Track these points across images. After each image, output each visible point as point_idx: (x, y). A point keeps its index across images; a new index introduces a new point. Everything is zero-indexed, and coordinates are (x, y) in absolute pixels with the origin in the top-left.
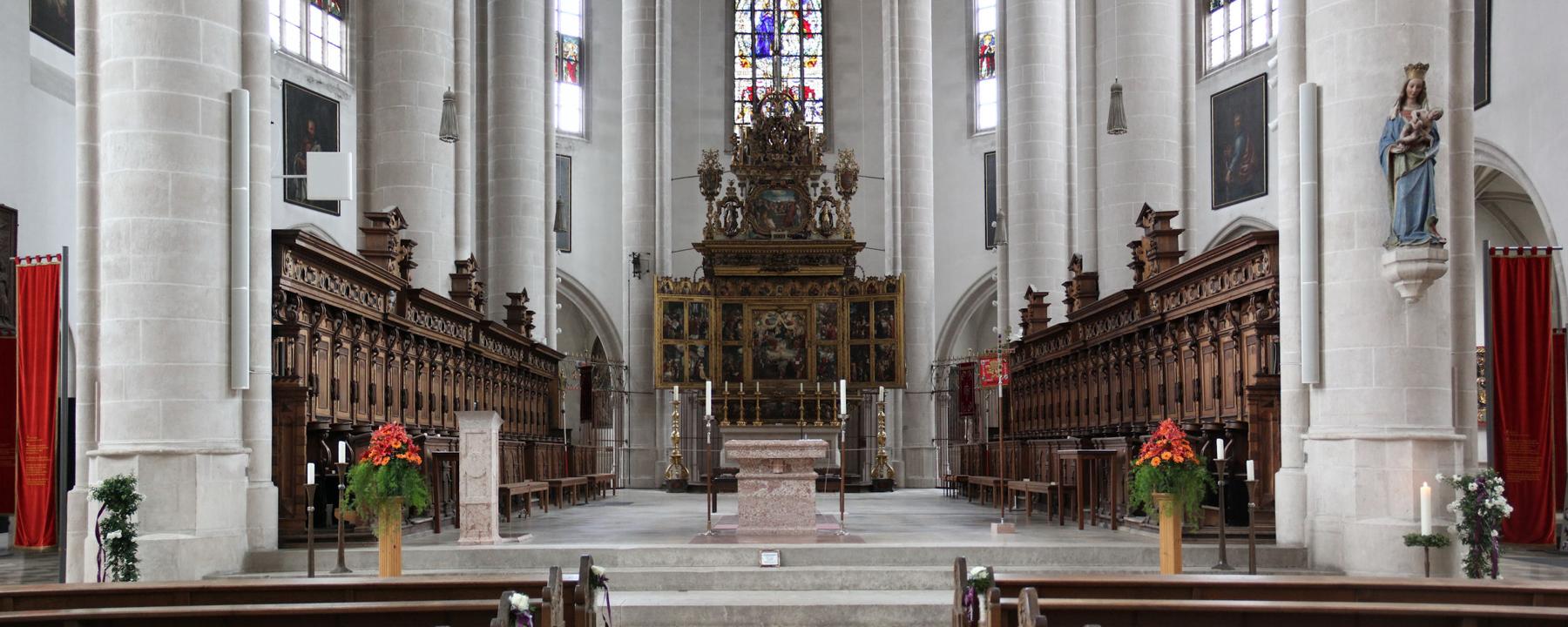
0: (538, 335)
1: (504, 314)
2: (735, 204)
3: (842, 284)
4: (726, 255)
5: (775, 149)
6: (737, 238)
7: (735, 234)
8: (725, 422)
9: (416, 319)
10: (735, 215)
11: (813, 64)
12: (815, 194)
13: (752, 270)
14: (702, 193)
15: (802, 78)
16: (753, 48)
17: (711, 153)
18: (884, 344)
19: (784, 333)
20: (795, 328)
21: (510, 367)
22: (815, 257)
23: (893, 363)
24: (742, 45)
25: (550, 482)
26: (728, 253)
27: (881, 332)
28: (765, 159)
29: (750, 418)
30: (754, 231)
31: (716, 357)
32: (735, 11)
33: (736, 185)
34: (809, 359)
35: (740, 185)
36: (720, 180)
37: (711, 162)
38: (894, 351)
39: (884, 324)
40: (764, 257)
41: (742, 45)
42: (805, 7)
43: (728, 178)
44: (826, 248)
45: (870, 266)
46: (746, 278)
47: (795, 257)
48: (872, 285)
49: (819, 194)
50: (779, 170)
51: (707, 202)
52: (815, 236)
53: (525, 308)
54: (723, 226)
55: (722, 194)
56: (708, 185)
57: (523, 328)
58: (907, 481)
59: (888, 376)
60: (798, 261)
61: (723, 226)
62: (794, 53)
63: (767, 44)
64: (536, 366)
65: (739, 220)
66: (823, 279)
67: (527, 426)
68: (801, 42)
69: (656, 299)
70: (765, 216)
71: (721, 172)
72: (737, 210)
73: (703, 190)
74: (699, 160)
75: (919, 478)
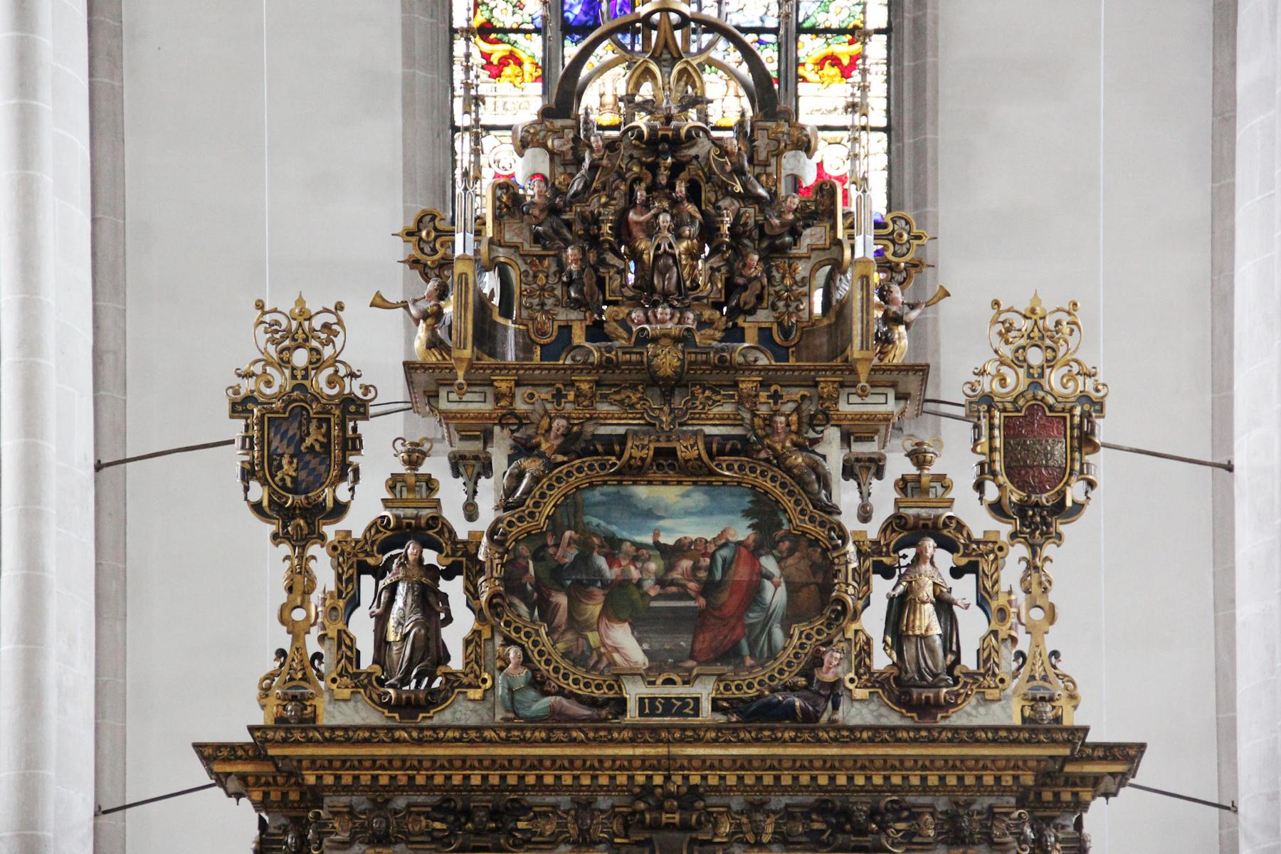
2: (430, 557)
4: (380, 798)
6: (444, 717)
7: (433, 700)
14: (257, 508)
22: (861, 807)
26: (394, 788)
28: (596, 332)
30: (538, 684)
33: (437, 466)
35: (457, 464)
36: (353, 444)
37: (300, 358)
40: (585, 807)
44: (926, 765)
47: (757, 807)
49: (884, 507)
51: (285, 549)
54: (366, 662)
56: (288, 468)
61: (366, 662)
65: (454, 637)
70: (594, 609)
71: (355, 407)
72: (444, 585)
73: (258, 492)
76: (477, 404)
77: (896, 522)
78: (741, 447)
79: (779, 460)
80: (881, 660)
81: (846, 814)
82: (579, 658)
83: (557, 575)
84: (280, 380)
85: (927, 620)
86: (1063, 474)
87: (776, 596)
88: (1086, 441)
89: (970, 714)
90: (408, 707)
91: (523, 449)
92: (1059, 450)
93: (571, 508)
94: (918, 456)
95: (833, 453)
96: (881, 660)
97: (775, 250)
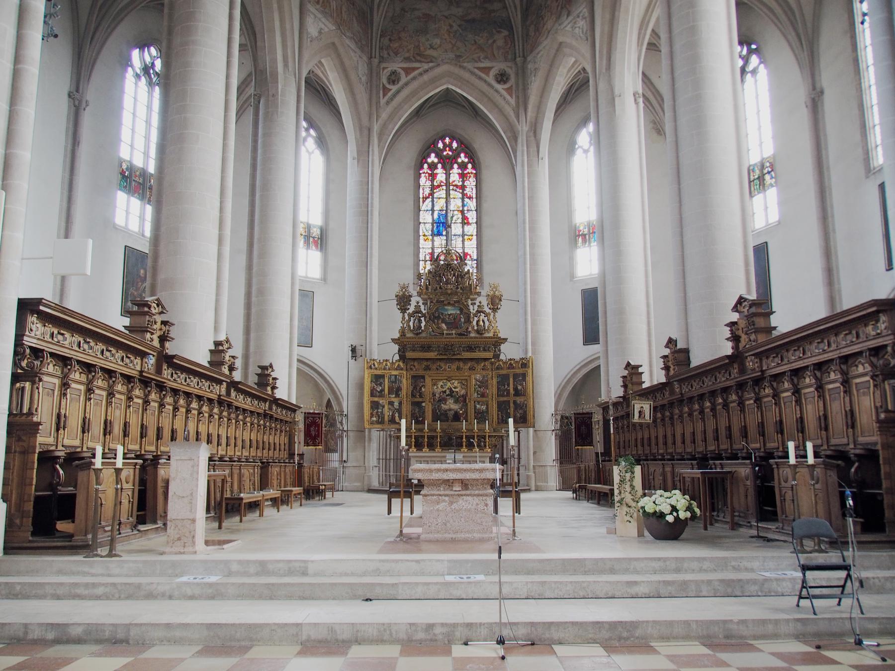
0: (281, 393)
1: (256, 379)
3: (492, 363)
5: (447, 283)
6: (420, 335)
7: (420, 333)
8: (413, 449)
9: (209, 388)
10: (420, 321)
11: (471, 240)
12: (473, 309)
13: (432, 355)
15: (463, 247)
16: (432, 230)
17: (404, 285)
18: (519, 400)
19: (451, 394)
20: (460, 390)
21: (258, 413)
23: (525, 412)
24: (426, 228)
25: (282, 491)
27: (517, 393)
29: (431, 447)
30: (433, 331)
31: (406, 408)
32: (420, 210)
33: (420, 304)
34: (469, 411)
36: (410, 301)
39: (519, 387)
41: (426, 228)
42: (466, 208)
43: (414, 301)
45: (508, 352)
46: (427, 360)
48: (510, 364)
50: (449, 295)
52: (473, 335)
53: (269, 375)
55: (412, 309)
57: (269, 388)
58: (536, 486)
60: (462, 349)
62: (459, 233)
63: (441, 228)
64: (277, 412)
65: (423, 324)
66: (478, 360)
67: (271, 452)
68: (463, 227)
69: (366, 373)
74: (396, 290)
75: (544, 484)
76: (426, 297)
77: (477, 311)
78: (458, 302)
79: (463, 303)
80: (476, 328)
81: (471, 347)
82: (438, 328)
83: (435, 317)
84: (401, 293)
85: (481, 323)
86: (498, 304)
87: (463, 320)
88: (500, 300)
89: (487, 335)
90: (417, 334)
91: (431, 302)
92: (497, 301)
93: (437, 309)
94: (480, 302)
95: (470, 302)
96: (476, 328)
97: (462, 278)
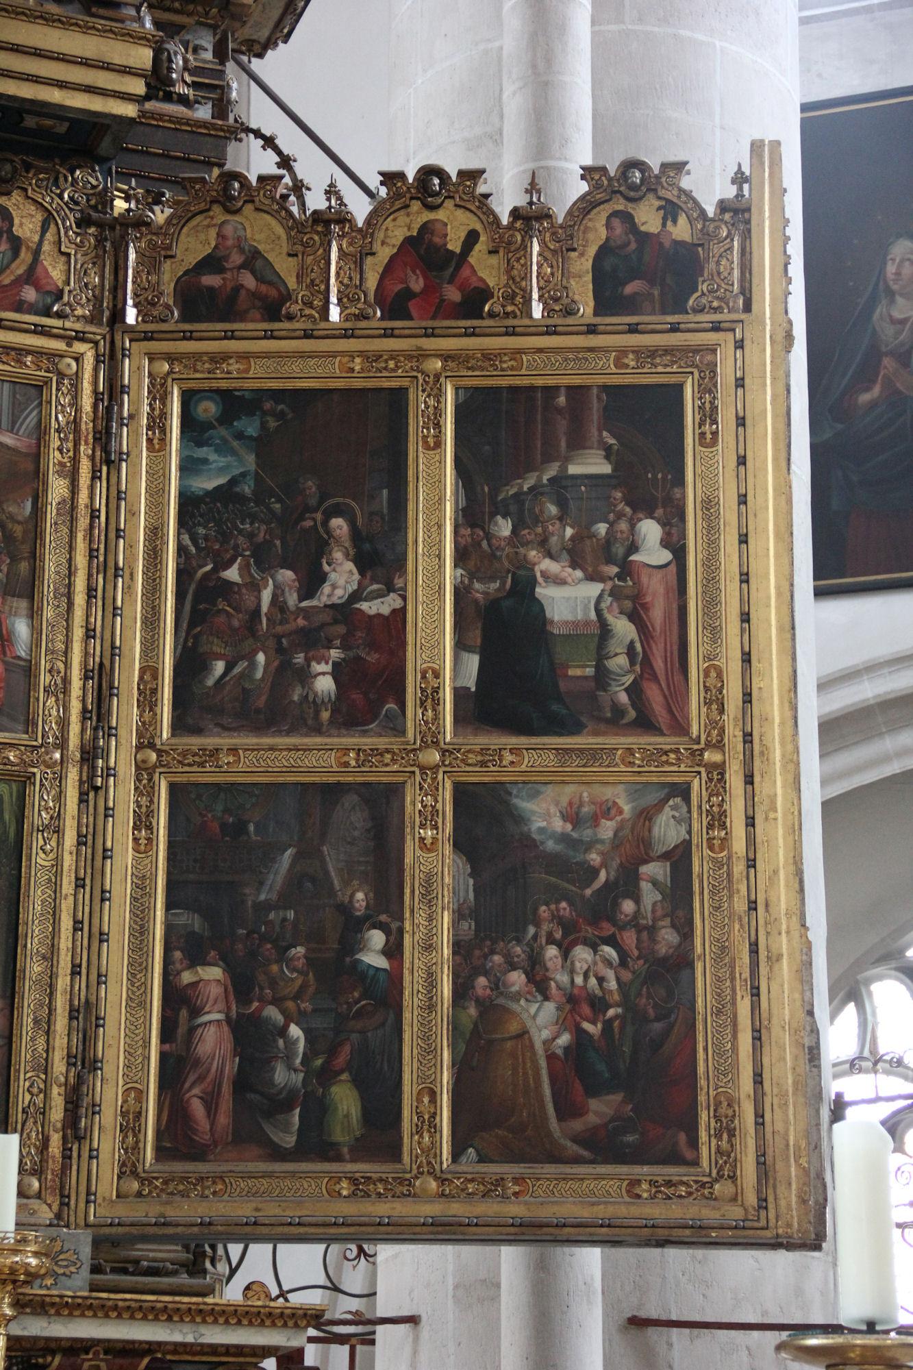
38: (680, 858)
59: (600, 1109)
